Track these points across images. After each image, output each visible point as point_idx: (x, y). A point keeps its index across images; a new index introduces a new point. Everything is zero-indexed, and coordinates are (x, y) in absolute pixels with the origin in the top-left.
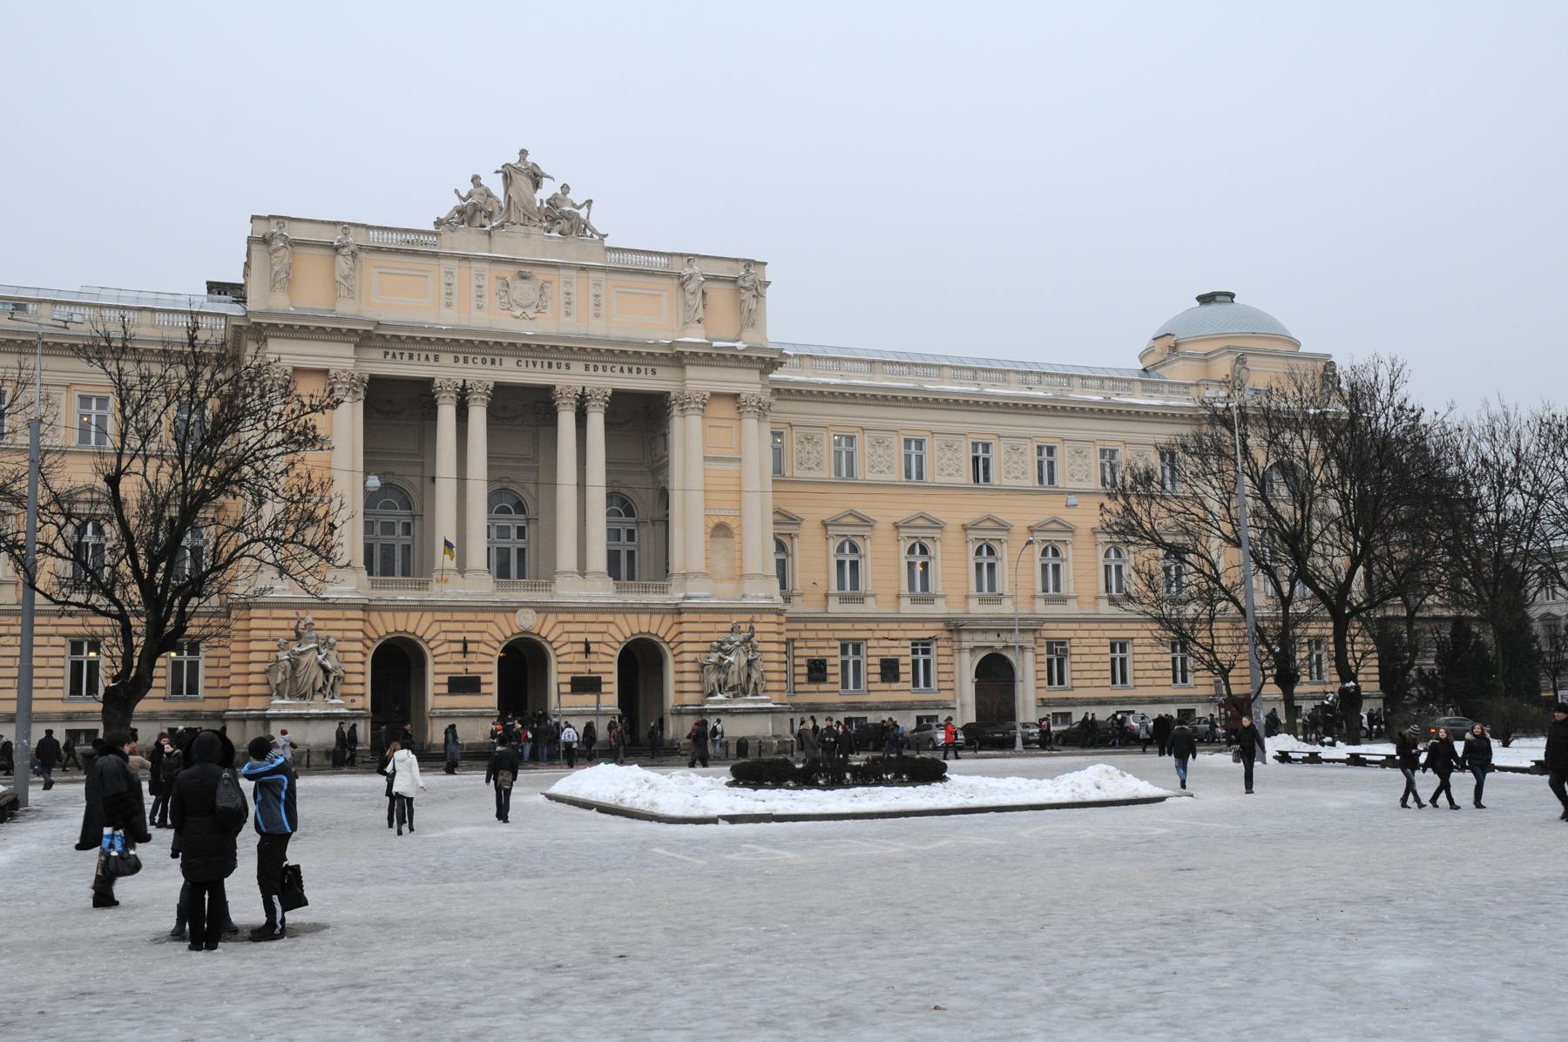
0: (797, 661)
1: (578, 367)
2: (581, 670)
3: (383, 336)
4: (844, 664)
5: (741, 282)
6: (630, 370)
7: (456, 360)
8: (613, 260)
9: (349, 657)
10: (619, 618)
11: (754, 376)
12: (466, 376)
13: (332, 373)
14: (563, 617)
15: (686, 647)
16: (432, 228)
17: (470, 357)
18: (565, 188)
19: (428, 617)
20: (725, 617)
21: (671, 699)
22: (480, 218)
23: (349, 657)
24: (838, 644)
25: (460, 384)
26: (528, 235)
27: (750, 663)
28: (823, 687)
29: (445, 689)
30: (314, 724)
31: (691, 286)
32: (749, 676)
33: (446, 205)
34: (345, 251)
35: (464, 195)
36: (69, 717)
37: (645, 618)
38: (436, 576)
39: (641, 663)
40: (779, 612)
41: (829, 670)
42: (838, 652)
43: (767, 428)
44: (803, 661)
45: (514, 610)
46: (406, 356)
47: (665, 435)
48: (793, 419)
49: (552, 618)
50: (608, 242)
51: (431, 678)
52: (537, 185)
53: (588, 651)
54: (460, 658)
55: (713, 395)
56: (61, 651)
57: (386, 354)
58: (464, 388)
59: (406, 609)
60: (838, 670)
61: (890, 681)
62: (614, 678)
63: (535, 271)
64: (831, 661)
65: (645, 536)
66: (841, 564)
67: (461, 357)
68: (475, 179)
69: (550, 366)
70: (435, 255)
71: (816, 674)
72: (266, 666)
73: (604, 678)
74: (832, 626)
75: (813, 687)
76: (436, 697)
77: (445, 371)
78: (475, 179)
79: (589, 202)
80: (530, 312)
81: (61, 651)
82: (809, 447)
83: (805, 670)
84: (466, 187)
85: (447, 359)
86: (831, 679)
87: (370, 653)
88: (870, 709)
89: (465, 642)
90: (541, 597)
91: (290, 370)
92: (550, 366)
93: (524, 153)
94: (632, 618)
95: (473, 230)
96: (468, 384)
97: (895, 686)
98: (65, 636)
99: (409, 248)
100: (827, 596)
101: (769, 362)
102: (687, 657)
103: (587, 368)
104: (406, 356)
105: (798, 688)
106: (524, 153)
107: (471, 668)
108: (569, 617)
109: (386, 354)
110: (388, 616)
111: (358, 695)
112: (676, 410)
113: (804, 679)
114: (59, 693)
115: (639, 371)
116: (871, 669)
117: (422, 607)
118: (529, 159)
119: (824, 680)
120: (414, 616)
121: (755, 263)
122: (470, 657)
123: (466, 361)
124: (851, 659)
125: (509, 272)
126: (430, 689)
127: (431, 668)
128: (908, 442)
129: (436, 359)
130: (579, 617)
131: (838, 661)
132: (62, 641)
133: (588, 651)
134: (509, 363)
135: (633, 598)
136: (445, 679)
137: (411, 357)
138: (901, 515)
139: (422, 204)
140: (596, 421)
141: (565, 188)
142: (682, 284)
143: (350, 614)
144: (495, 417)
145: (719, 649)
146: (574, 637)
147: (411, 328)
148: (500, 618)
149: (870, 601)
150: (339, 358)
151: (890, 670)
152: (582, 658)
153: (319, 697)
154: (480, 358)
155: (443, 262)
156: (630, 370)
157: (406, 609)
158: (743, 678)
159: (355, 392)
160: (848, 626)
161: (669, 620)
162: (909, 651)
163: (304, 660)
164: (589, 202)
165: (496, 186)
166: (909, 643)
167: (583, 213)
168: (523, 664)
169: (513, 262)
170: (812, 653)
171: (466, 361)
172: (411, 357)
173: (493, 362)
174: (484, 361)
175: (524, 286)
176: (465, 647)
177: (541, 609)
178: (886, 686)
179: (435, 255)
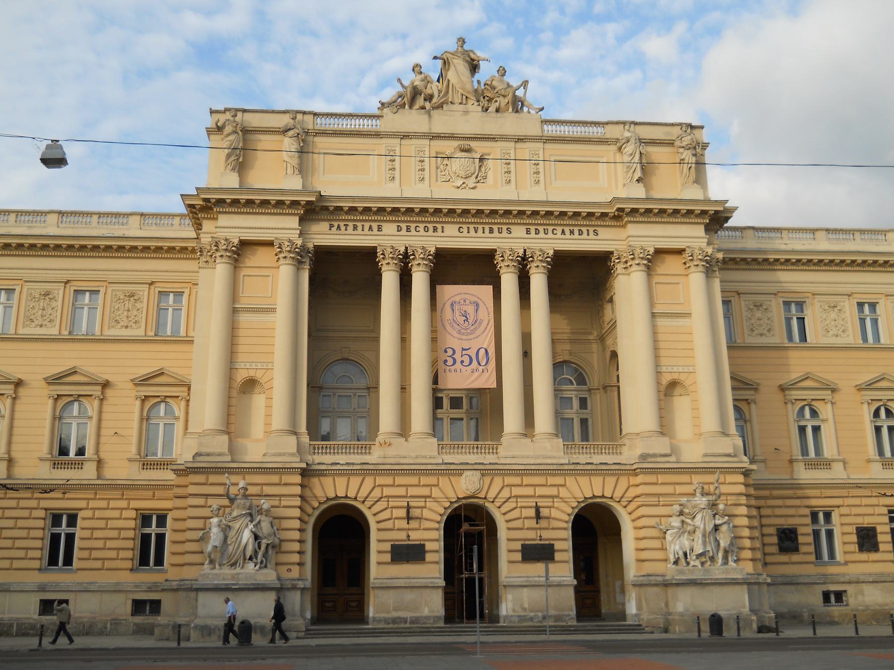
0: (766, 530)
1: (519, 231)
2: (531, 536)
3: (326, 208)
5: (677, 143)
6: (572, 232)
7: (399, 229)
8: (550, 130)
9: (287, 524)
10: (570, 481)
11: (700, 231)
12: (407, 243)
13: (276, 244)
14: (509, 480)
16: (377, 112)
17: (413, 226)
18: (502, 72)
19: (369, 482)
20: (685, 478)
22: (420, 101)
23: (287, 524)
24: (807, 511)
25: (402, 250)
26: (466, 112)
27: (716, 528)
28: (795, 558)
29: (388, 557)
30: (243, 594)
31: (629, 148)
34: (291, 133)
35: (406, 83)
36: (42, 588)
37: (597, 481)
38: (380, 438)
39: (595, 529)
40: (746, 473)
41: (801, 539)
42: (808, 520)
43: (717, 284)
44: (772, 530)
45: (459, 473)
46: (350, 228)
47: (611, 300)
48: (742, 288)
49: (498, 482)
50: (544, 115)
51: (374, 546)
52: (474, 67)
53: (538, 516)
54: (403, 524)
55: (659, 252)
56: (41, 523)
57: (331, 226)
58: (406, 255)
59: (348, 473)
60: (811, 539)
61: (869, 551)
62: (568, 545)
63: (473, 144)
64: (801, 530)
65: (597, 401)
66: (802, 429)
67: (404, 226)
69: (491, 231)
70: (377, 135)
71: (787, 544)
72: (201, 533)
73: (558, 545)
75: (784, 558)
76: (378, 567)
77: (388, 238)
80: (471, 182)
81: (41, 523)
82: (758, 314)
83: (775, 540)
84: (409, 79)
85: (389, 228)
86: (803, 549)
87: (312, 520)
88: (850, 583)
89: (408, 508)
90: (490, 458)
91: (236, 241)
92: (491, 231)
94: (584, 481)
95: (413, 111)
96: (410, 252)
97: (873, 556)
98: (46, 509)
99: (354, 130)
100: (791, 461)
101: (716, 219)
103: (528, 232)
104: (350, 228)
105: (769, 559)
106: (462, 41)
107: (414, 535)
108: (516, 480)
109: (331, 226)
110: (328, 481)
111: (299, 565)
112: (619, 271)
113: (775, 549)
114: (36, 564)
115: (581, 233)
116: (848, 538)
117: (365, 471)
118: (466, 47)
120: (355, 481)
121: (692, 127)
122: (414, 524)
123: (408, 229)
125: (448, 147)
126: (374, 557)
127: (374, 535)
128: (860, 305)
129: (380, 229)
130: (527, 480)
131: (809, 530)
132: (42, 514)
133: (538, 516)
134: (451, 229)
135: (583, 459)
136: (387, 547)
137: (355, 228)
138: (865, 377)
140: (538, 283)
141: (502, 72)
142: (620, 149)
143: (286, 479)
144: (436, 280)
146: (522, 502)
147: (353, 198)
148: (444, 481)
149: (838, 467)
150: (285, 228)
151: (867, 539)
152: (532, 523)
153: (250, 566)
154: (422, 226)
155: (384, 141)
156: (572, 232)
157: (348, 473)
159: (300, 262)
162: (886, 519)
163: (236, 525)
164: (525, 84)
166: (885, 510)
167: (520, 93)
168: (468, 533)
169: (452, 137)
170: (781, 521)
171: (408, 229)
172: (355, 228)
173: (435, 229)
174: (426, 229)
176: (408, 512)
177: (486, 472)
178: (864, 556)
179: (377, 135)
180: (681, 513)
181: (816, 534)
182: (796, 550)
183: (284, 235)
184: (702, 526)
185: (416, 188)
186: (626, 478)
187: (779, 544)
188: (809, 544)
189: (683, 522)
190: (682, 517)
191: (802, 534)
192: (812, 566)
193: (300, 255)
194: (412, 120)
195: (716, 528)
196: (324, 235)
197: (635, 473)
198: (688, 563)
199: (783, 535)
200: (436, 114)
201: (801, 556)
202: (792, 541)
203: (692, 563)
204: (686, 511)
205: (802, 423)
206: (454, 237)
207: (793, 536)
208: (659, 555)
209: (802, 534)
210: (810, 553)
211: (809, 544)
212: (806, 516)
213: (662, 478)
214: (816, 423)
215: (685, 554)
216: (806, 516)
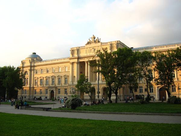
18: (98, 38)
28: (137, 92)
33: (86, 43)
36: (64, 96)
63: (94, 48)
68: (89, 39)
77: (86, 60)
78: (89, 39)
79: (100, 39)
84: (89, 41)
85: (86, 59)
93: (93, 35)
94: (103, 85)
124: (141, 88)
139: (83, 43)
141: (98, 38)
164: (100, 39)
165: (91, 40)
175: (93, 49)
181: (140, 89)
183: (76, 61)
185: (88, 54)
193: (78, 63)
194: (89, 46)
196: (81, 60)
200: (90, 45)
206: (91, 59)
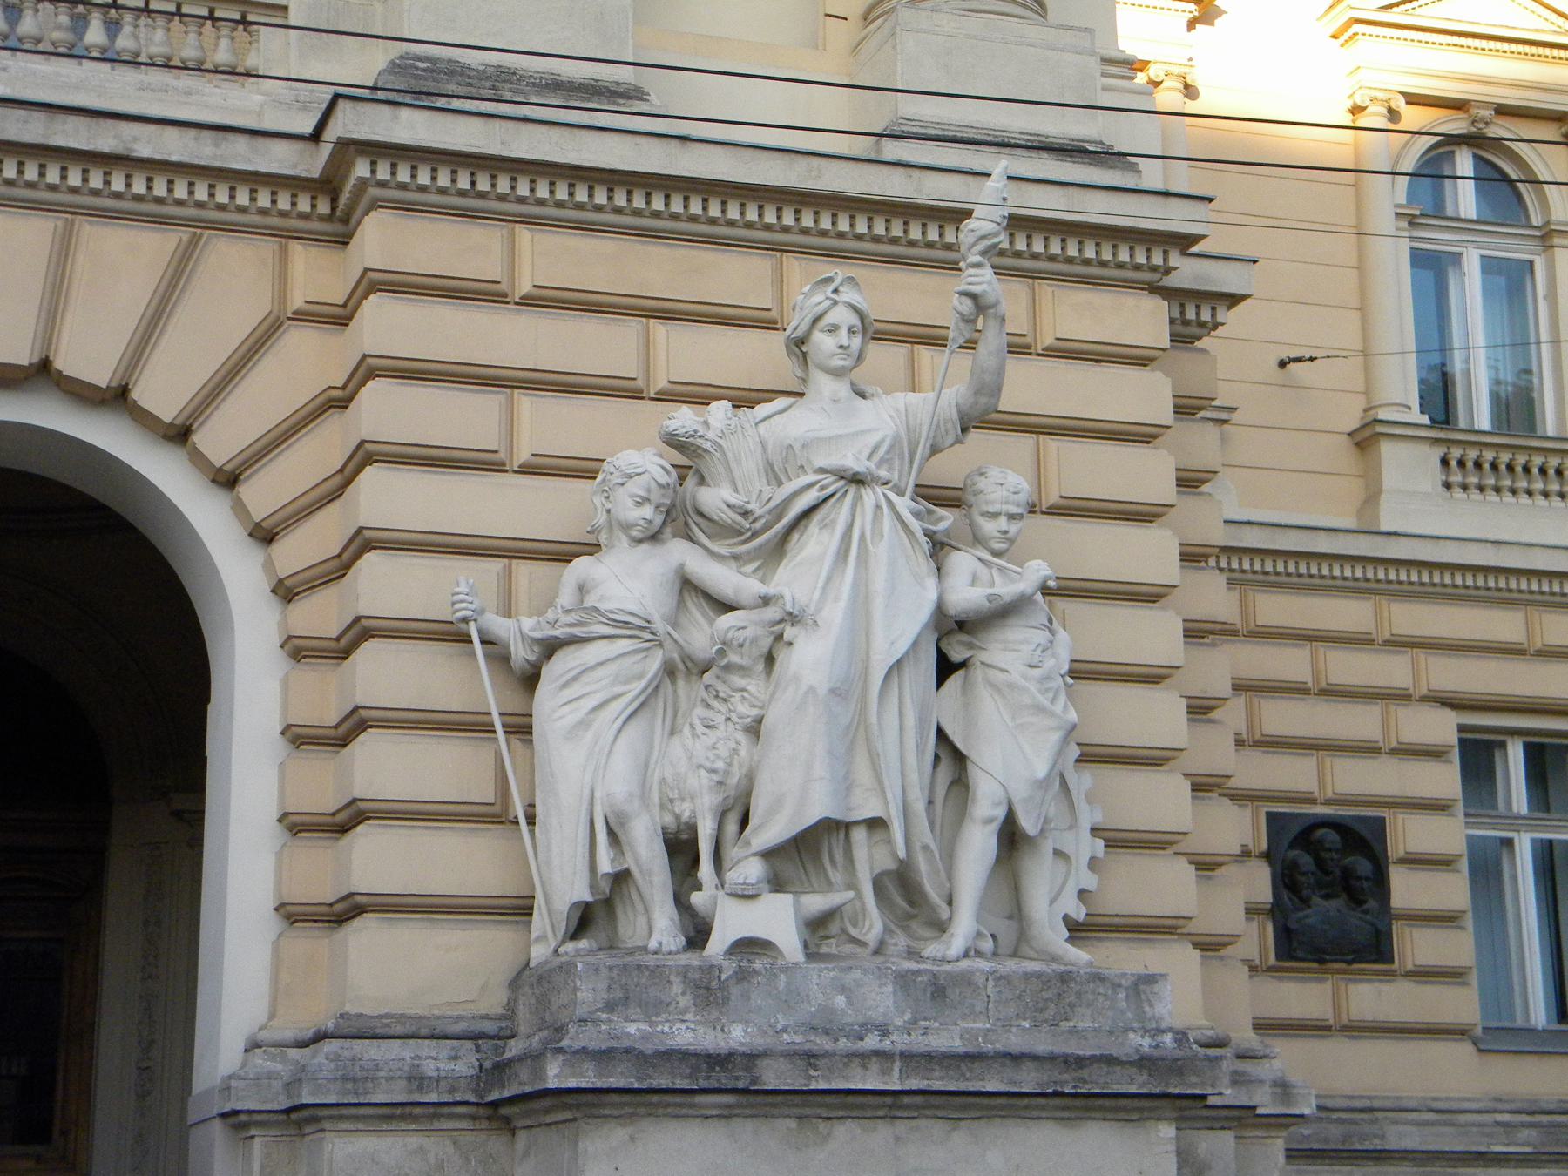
4: (1487, 868)
15: (385, 498)
20: (733, 277)
21: (247, 981)
24: (1442, 728)
27: (952, 645)
28: (1368, 997)
32: (950, 754)
41: (1406, 889)
42: (1445, 779)
60: (1453, 891)
64: (1409, 834)
74: (1411, 618)
86: (1417, 946)
102: (384, 585)
119: (1371, 948)
145: (677, 519)
158: (896, 781)
160: (1504, 625)
161: (236, 281)
180: (677, 519)
182: (1371, 948)
184: (834, 614)
186: (266, 248)
187: (1276, 911)
188: (1448, 919)
189: (687, 586)
190: (678, 552)
191: (1415, 861)
192: (1465, 1049)
195: (952, 645)
197: (331, 196)
198: (697, 932)
199: (1306, 860)
201: (1405, 987)
202: (1356, 899)
203: (732, 922)
204: (715, 498)
205: (1436, 239)
207: (1363, 866)
208: (460, 862)
209: (1415, 861)
210: (1451, 975)
211: (1448, 919)
212: (1433, 753)
213: (547, 257)
214: (1513, 249)
215: (681, 849)
216: (1433, 753)
